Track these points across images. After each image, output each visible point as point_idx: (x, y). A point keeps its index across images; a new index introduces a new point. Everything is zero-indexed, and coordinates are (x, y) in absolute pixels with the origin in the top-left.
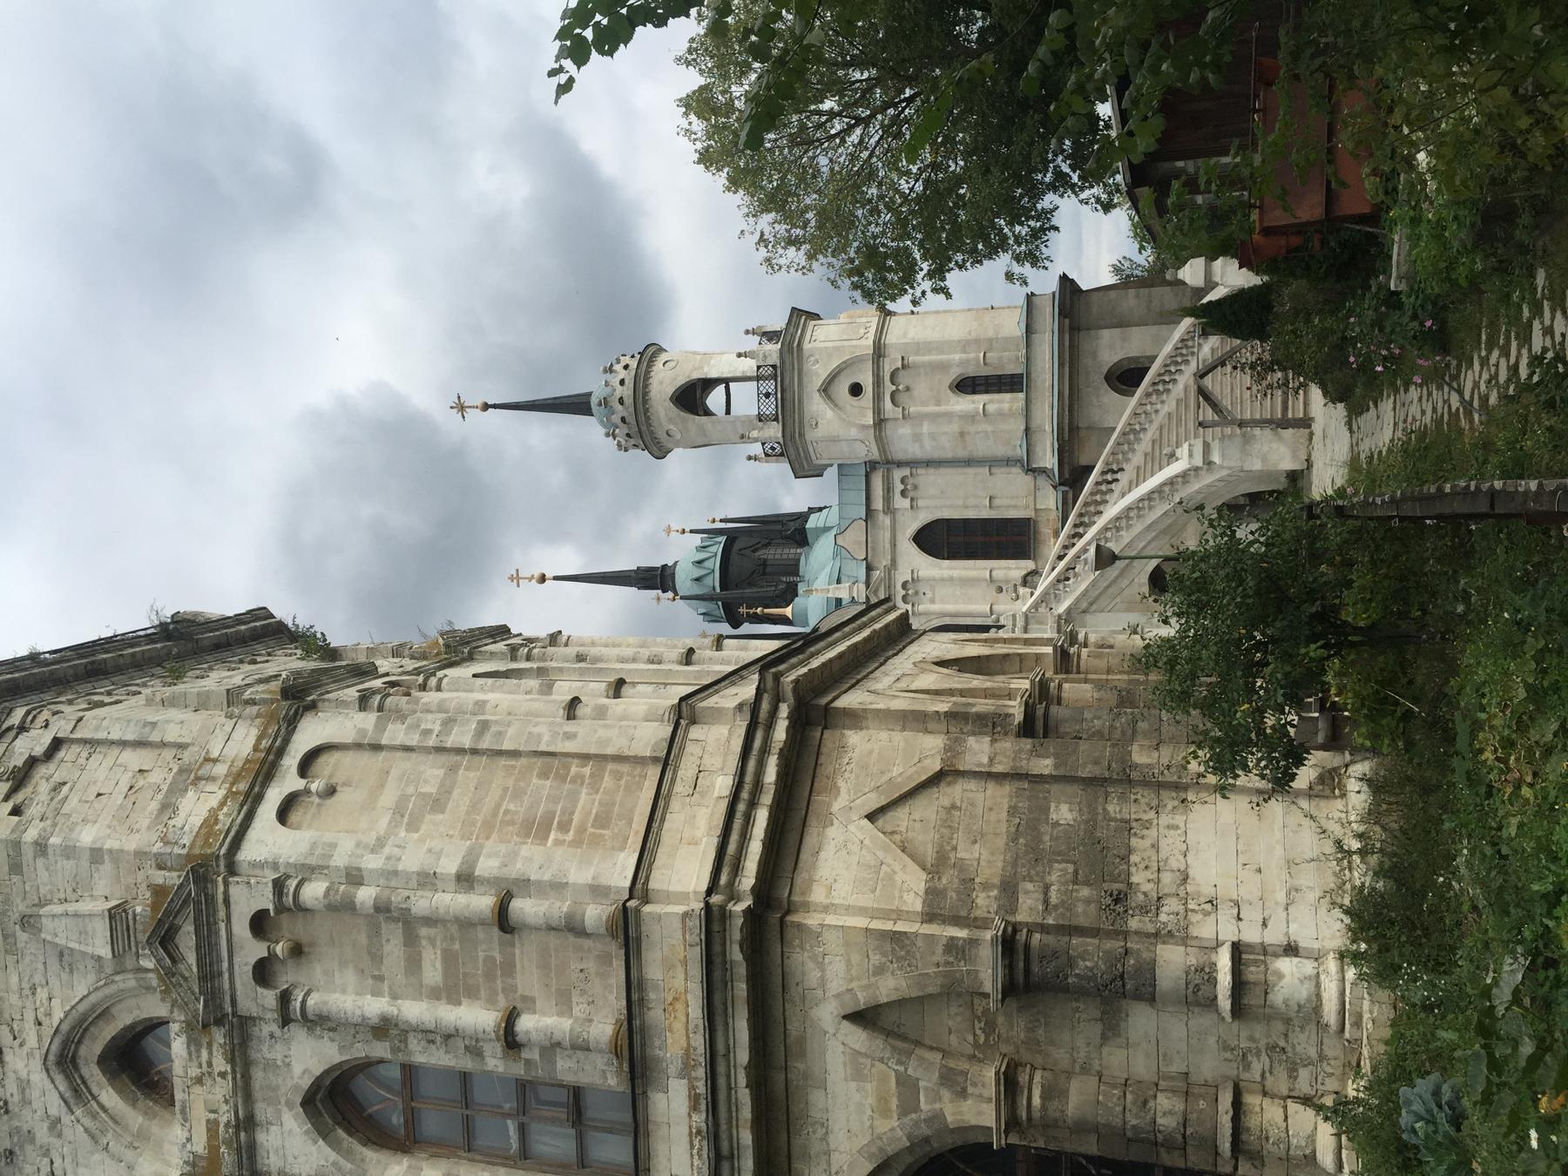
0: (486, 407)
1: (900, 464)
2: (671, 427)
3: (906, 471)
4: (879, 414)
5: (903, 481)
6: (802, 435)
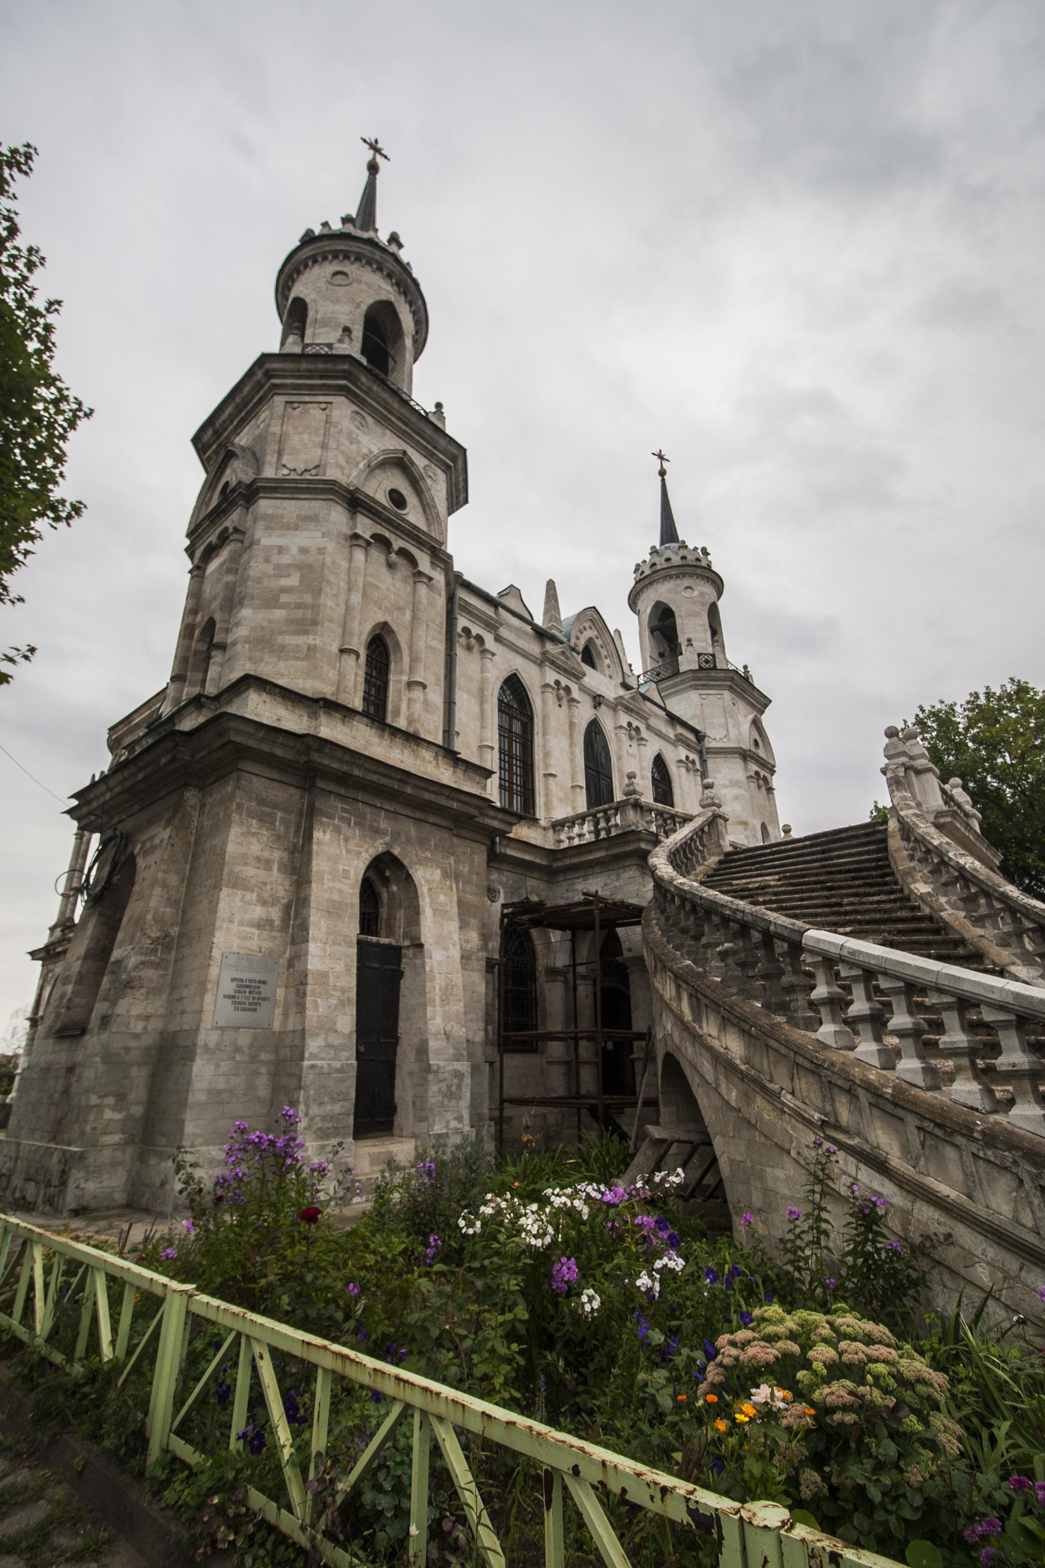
0: (662, 473)
1: (703, 762)
2: (696, 593)
3: (698, 766)
4: (752, 758)
5: (693, 762)
6: (731, 689)
